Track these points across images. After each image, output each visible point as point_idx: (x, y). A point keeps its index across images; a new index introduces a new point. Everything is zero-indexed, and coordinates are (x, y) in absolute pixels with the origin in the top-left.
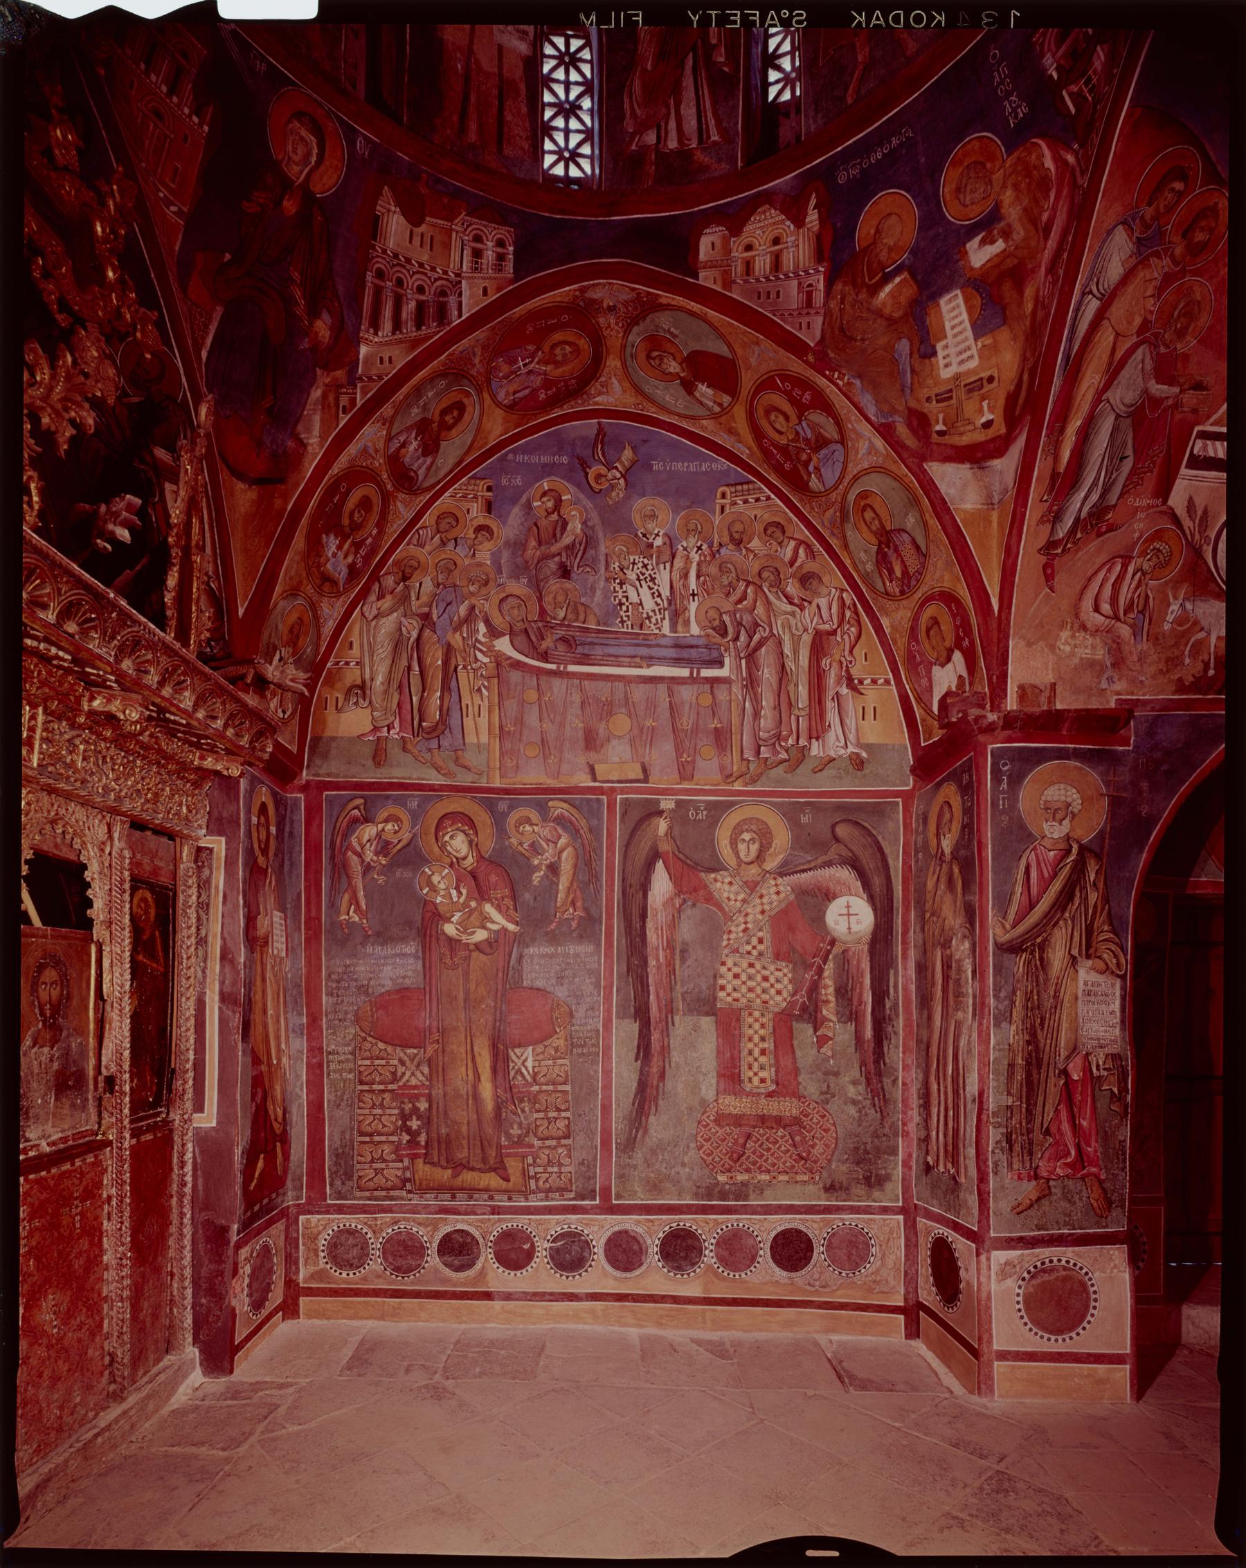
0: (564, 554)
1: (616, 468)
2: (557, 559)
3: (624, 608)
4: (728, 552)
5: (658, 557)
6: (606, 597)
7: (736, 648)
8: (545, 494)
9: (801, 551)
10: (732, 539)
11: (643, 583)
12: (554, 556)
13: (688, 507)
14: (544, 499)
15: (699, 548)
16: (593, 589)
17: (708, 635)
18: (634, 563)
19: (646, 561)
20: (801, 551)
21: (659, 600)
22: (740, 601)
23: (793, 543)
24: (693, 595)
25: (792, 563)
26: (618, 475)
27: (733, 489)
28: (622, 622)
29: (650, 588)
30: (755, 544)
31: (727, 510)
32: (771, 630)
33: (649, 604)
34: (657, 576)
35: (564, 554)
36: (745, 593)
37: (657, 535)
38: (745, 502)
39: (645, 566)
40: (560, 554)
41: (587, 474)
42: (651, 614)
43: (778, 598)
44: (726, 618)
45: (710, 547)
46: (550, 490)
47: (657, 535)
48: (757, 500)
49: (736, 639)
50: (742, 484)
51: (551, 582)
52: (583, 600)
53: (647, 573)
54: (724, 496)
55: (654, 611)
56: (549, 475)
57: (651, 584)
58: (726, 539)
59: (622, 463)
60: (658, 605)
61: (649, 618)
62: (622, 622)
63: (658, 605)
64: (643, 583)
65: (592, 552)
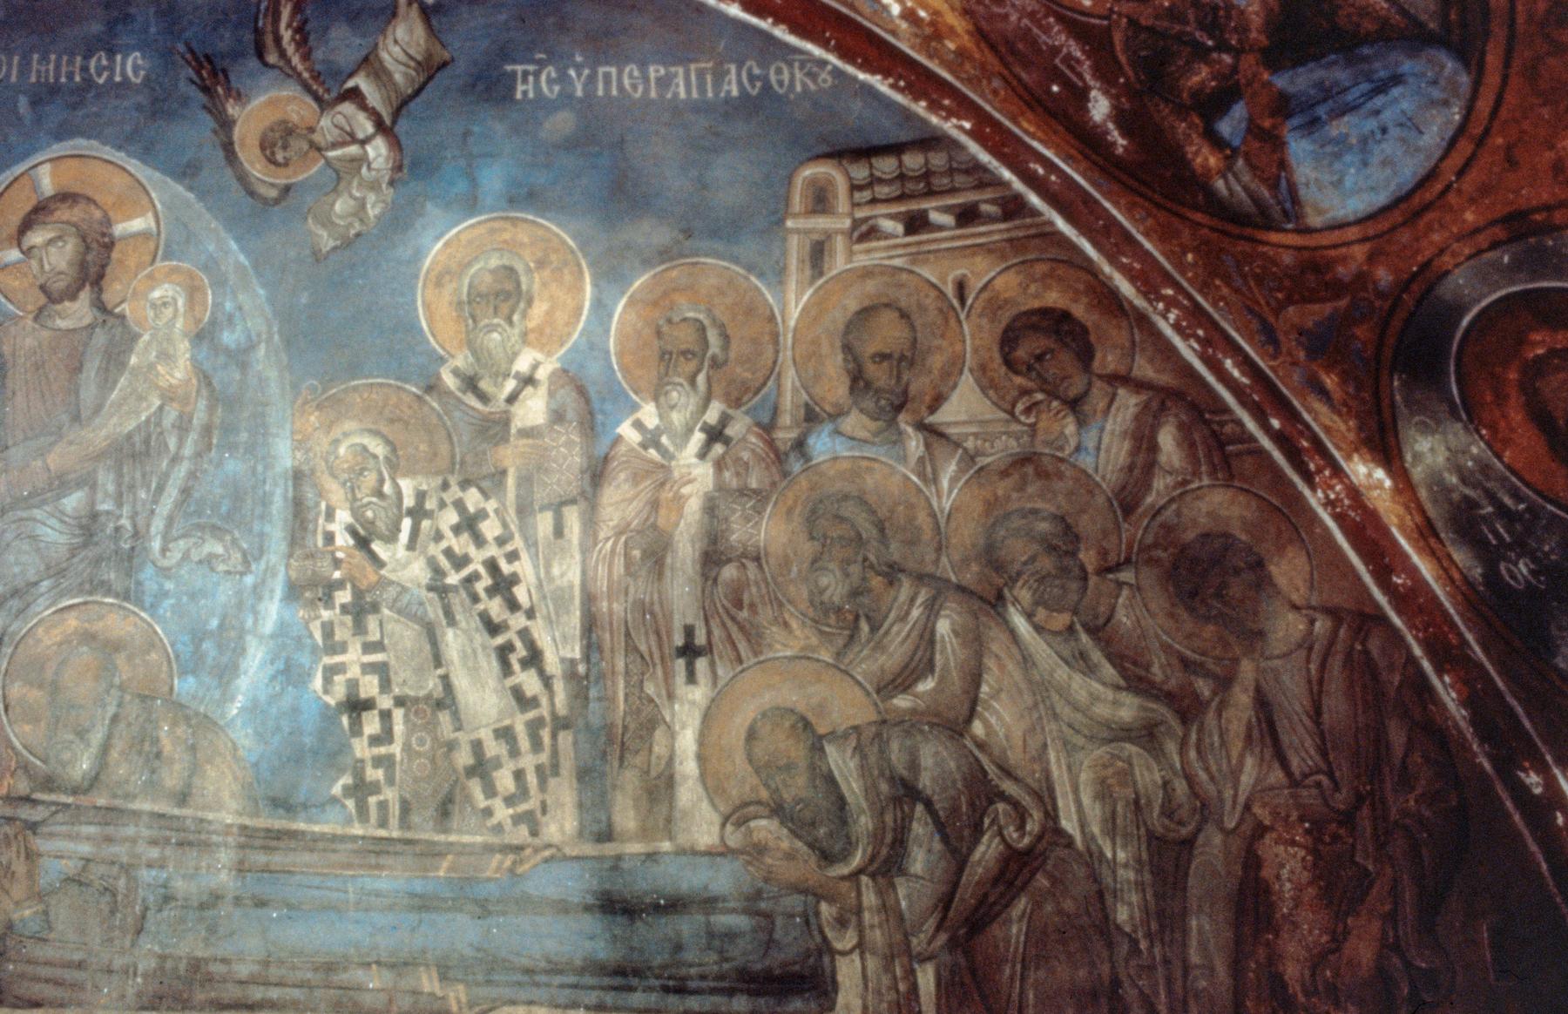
0: (106, 480)
1: (354, 95)
2: (73, 501)
3: (372, 725)
4: (842, 449)
5: (525, 481)
6: (290, 674)
7: (888, 909)
8: (38, 213)
9: (1167, 439)
10: (858, 381)
11: (458, 601)
12: (61, 484)
13: (665, 255)
14: (36, 238)
15: (715, 435)
16: (231, 640)
17: (757, 851)
18: (418, 513)
19: (473, 499)
20: (1167, 439)
21: (530, 682)
22: (903, 680)
23: (1128, 403)
24: (689, 651)
25: (1127, 501)
26: (366, 126)
27: (860, 172)
28: (361, 789)
29: (493, 628)
30: (964, 406)
31: (839, 262)
32: (1051, 815)
33: (483, 698)
34: (524, 567)
35: (106, 480)
36: (927, 638)
37: (528, 381)
38: (916, 223)
39: (469, 524)
40: (88, 482)
41: (226, 124)
42: (493, 748)
43: (1080, 662)
44: (841, 762)
45: (767, 428)
46: (66, 197)
47: (528, 381)
48: (967, 216)
49: (888, 864)
50: (896, 149)
51: (43, 609)
52: (185, 686)
53: (478, 557)
54: (820, 201)
55: (505, 734)
56: (61, 134)
57: (495, 607)
58: (835, 388)
59: (380, 74)
60: (523, 700)
61: (481, 768)
62: (361, 789)
63: (523, 700)
64: (458, 601)
65: (234, 466)
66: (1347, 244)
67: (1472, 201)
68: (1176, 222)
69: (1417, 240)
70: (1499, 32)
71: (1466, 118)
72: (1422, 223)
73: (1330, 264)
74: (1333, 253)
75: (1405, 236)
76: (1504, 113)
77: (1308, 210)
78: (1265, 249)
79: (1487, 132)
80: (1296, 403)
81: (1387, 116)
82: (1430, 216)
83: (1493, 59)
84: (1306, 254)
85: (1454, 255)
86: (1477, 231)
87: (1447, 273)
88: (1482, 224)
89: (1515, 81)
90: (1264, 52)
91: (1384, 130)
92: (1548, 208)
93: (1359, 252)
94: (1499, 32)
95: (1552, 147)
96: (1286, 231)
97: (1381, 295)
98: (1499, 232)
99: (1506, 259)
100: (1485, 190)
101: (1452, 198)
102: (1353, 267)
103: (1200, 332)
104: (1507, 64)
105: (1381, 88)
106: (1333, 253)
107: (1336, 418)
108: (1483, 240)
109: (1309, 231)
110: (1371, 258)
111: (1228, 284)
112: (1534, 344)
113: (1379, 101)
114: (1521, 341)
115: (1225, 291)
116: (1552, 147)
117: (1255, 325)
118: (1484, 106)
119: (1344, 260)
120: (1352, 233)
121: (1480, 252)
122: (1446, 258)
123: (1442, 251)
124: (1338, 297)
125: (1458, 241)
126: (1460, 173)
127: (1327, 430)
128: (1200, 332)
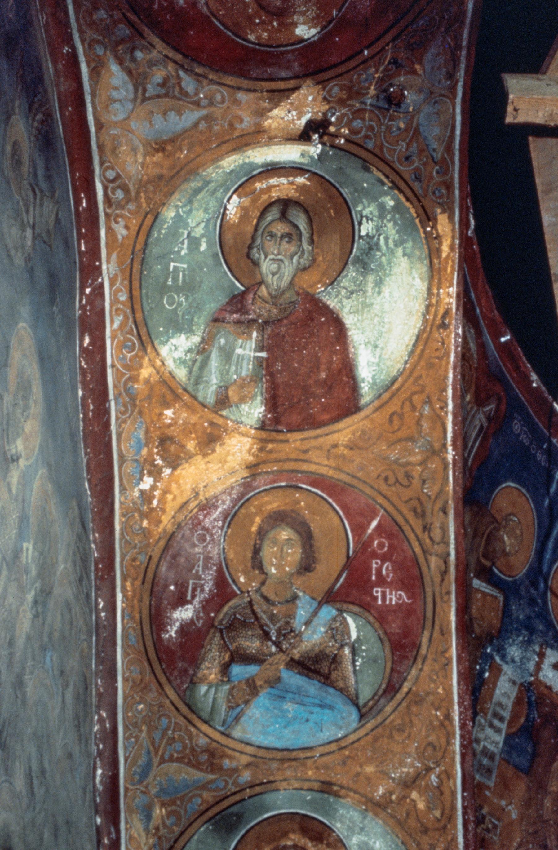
66: (241, 752)
67: (317, 768)
68: (154, 686)
69: (278, 769)
70: (379, 719)
71: (343, 737)
72: (286, 765)
73: (224, 756)
74: (230, 752)
75: (275, 765)
76: (355, 745)
77: (239, 728)
78: (193, 730)
79: (346, 747)
80: (122, 815)
81: (314, 716)
82: (293, 763)
83: (369, 726)
84: (214, 745)
85: (288, 784)
86: (309, 780)
87: (278, 790)
88: (312, 778)
89: (369, 738)
90: (292, 660)
91: (307, 721)
92: (342, 787)
93: (245, 759)
94: (379, 719)
95: (361, 766)
96: (215, 729)
97: (235, 783)
98: (316, 786)
99: (309, 798)
100: (326, 767)
101: (310, 762)
102: (234, 764)
103: (101, 746)
104: (372, 730)
105: (322, 706)
106: (230, 752)
107: (143, 834)
108: (307, 785)
109: (228, 736)
110: (248, 765)
111: (149, 732)
112: (290, 839)
113: (316, 709)
114: (285, 834)
115: (144, 735)
116: (361, 766)
117: (143, 761)
118: (353, 737)
119: (231, 758)
120: (249, 749)
121: (301, 789)
122: (284, 784)
123: (285, 780)
124: (212, 772)
125: (296, 780)
126: (322, 755)
127: (130, 838)
128: (101, 746)
